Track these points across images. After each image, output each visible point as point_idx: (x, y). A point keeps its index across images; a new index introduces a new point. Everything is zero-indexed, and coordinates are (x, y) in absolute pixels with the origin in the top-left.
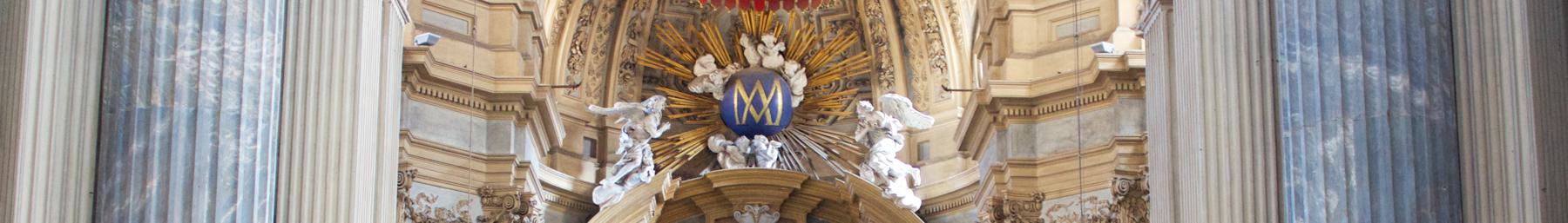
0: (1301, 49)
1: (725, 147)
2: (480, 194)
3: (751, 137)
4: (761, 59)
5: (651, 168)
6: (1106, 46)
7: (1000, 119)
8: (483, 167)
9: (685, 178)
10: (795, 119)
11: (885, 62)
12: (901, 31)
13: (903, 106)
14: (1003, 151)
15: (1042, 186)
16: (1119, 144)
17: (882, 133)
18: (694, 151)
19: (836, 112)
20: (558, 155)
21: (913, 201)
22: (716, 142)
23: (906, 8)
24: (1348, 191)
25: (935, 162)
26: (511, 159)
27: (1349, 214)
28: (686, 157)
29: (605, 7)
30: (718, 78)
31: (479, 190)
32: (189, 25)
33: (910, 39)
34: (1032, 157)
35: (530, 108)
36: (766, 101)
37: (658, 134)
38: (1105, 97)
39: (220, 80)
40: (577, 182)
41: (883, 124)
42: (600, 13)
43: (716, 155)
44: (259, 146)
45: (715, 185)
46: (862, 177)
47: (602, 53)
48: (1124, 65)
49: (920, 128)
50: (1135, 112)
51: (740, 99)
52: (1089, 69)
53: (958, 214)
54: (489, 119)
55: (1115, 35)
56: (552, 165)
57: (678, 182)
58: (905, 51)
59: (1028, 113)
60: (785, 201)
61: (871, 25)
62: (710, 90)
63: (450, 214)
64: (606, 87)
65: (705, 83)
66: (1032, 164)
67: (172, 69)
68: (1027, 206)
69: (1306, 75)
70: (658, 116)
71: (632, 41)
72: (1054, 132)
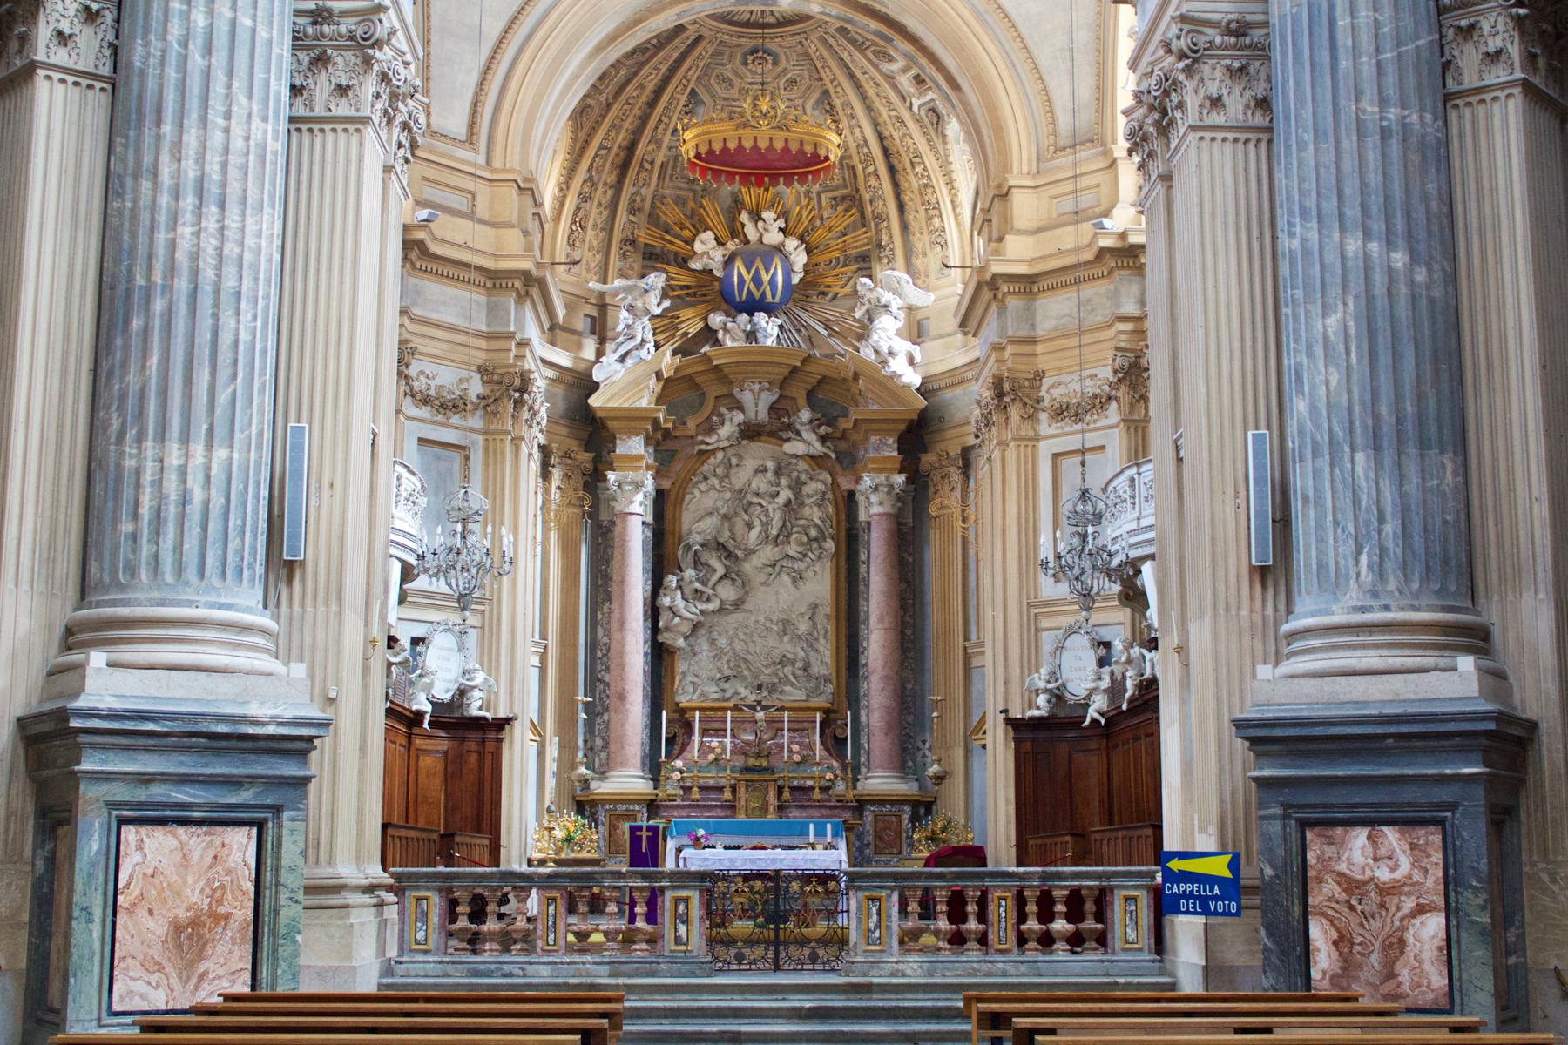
0: (1301, 225)
1: (725, 324)
2: (480, 372)
3: (751, 314)
4: (761, 236)
5: (651, 346)
6: (1106, 222)
7: (1000, 296)
8: (483, 344)
9: (685, 355)
10: (796, 296)
11: (885, 238)
12: (901, 208)
13: (903, 282)
14: (1003, 329)
15: (1042, 363)
17: (882, 310)
18: (694, 328)
19: (837, 289)
20: (558, 332)
21: (913, 378)
22: (716, 319)
23: (906, 185)
24: (1348, 368)
25: (934, 339)
26: (511, 336)
27: (1349, 391)
28: (686, 334)
29: (605, 183)
30: (718, 255)
31: (479, 367)
32: (189, 201)
33: (910, 216)
34: (1032, 334)
35: (530, 285)
36: (766, 278)
37: (658, 311)
39: (220, 256)
40: (577, 359)
41: (883, 301)
42: (600, 189)
43: (716, 332)
44: (259, 323)
45: (715, 363)
46: (862, 354)
47: (602, 229)
49: (920, 305)
50: (1135, 289)
51: (740, 276)
52: (1089, 245)
53: (958, 391)
54: (489, 296)
55: (1115, 211)
56: (553, 343)
57: (678, 359)
58: (905, 227)
60: (785, 378)
61: (871, 201)
62: (710, 267)
63: (450, 392)
64: (606, 264)
65: (705, 260)
66: (1033, 341)
67: (172, 245)
68: (1027, 384)
69: (1306, 252)
70: (658, 293)
71: (632, 218)
72: (1054, 309)
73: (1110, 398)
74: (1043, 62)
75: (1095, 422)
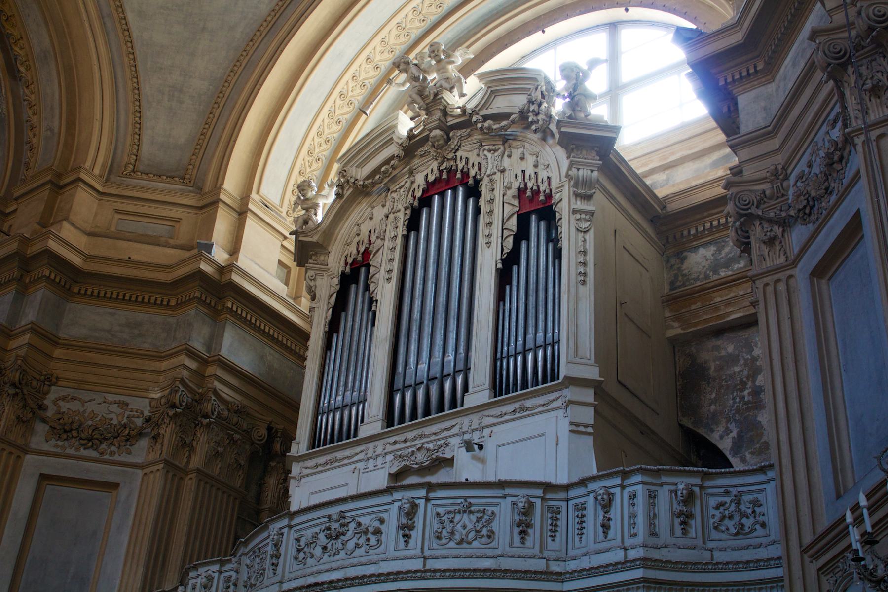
16: (187, 354)
38: (173, 303)
48: (221, 277)
50: (206, 331)
59: (67, 286)
68: (34, 383)
73: (140, 434)
74: (147, 89)
75: (112, 454)
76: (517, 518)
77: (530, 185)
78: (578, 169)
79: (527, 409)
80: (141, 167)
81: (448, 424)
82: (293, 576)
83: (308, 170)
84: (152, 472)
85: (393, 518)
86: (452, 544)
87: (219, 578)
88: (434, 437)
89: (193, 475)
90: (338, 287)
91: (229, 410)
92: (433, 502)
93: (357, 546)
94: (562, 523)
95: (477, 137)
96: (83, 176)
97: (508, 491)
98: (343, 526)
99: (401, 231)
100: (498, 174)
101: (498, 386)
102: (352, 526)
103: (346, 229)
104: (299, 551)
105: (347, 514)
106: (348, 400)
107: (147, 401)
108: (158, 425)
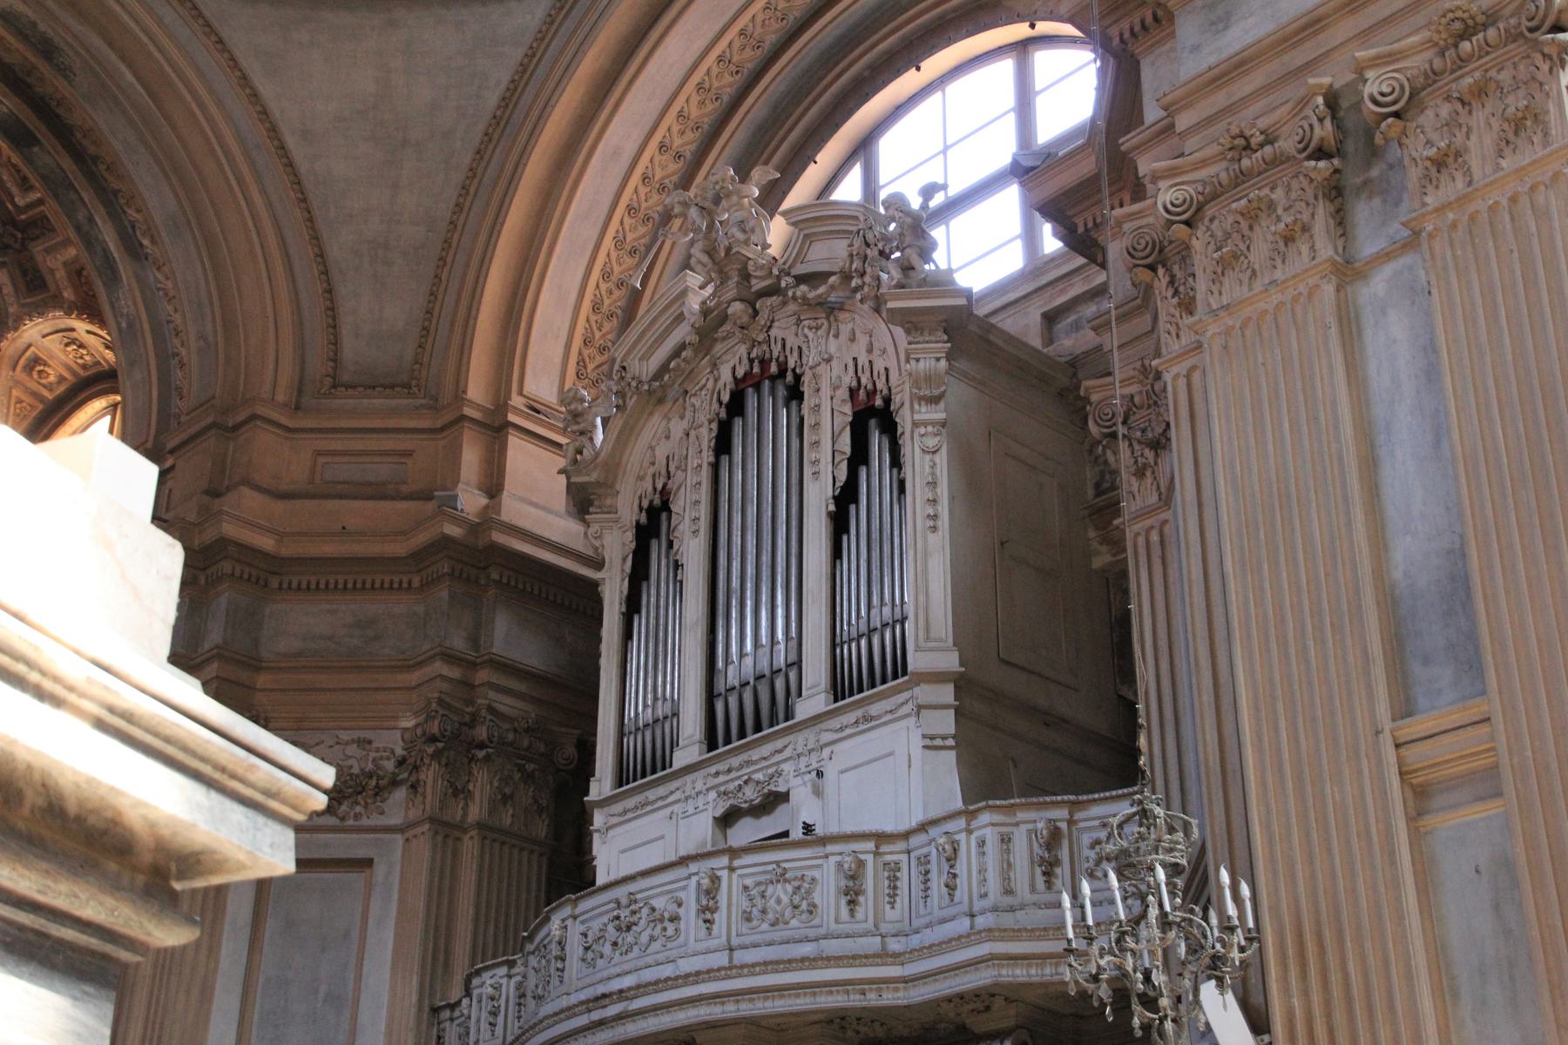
16: (442, 660)
73: (395, 783)
74: (334, 251)
75: (357, 817)
76: (843, 883)
77: (864, 381)
78: (918, 360)
79: (872, 718)
80: (345, 377)
81: (779, 744)
82: (580, 985)
83: (598, 335)
84: (415, 836)
85: (690, 898)
86: (765, 926)
87: (508, 985)
88: (764, 764)
89: (474, 833)
90: (633, 545)
91: (515, 730)
92: (739, 872)
93: (652, 939)
94: (903, 884)
95: (792, 307)
96: (260, 410)
97: (830, 848)
98: (634, 913)
99: (708, 456)
100: (823, 364)
101: (840, 687)
102: (645, 911)
103: (636, 455)
104: (587, 949)
105: (638, 896)
106: (660, 713)
107: (398, 734)
108: (416, 768)
